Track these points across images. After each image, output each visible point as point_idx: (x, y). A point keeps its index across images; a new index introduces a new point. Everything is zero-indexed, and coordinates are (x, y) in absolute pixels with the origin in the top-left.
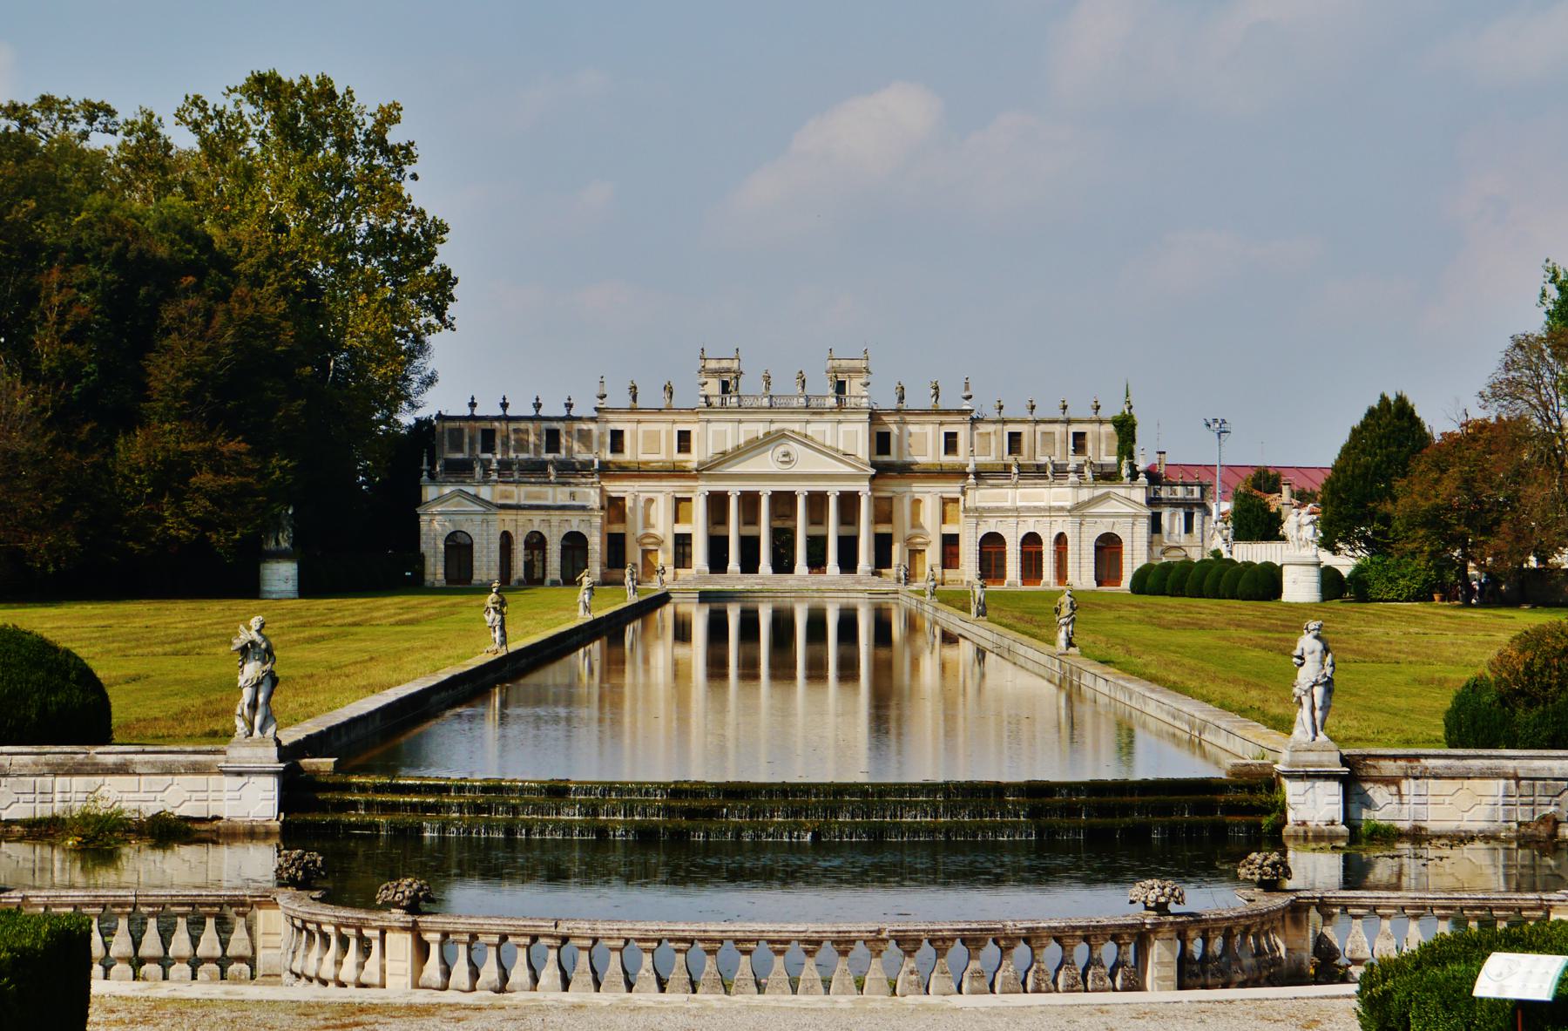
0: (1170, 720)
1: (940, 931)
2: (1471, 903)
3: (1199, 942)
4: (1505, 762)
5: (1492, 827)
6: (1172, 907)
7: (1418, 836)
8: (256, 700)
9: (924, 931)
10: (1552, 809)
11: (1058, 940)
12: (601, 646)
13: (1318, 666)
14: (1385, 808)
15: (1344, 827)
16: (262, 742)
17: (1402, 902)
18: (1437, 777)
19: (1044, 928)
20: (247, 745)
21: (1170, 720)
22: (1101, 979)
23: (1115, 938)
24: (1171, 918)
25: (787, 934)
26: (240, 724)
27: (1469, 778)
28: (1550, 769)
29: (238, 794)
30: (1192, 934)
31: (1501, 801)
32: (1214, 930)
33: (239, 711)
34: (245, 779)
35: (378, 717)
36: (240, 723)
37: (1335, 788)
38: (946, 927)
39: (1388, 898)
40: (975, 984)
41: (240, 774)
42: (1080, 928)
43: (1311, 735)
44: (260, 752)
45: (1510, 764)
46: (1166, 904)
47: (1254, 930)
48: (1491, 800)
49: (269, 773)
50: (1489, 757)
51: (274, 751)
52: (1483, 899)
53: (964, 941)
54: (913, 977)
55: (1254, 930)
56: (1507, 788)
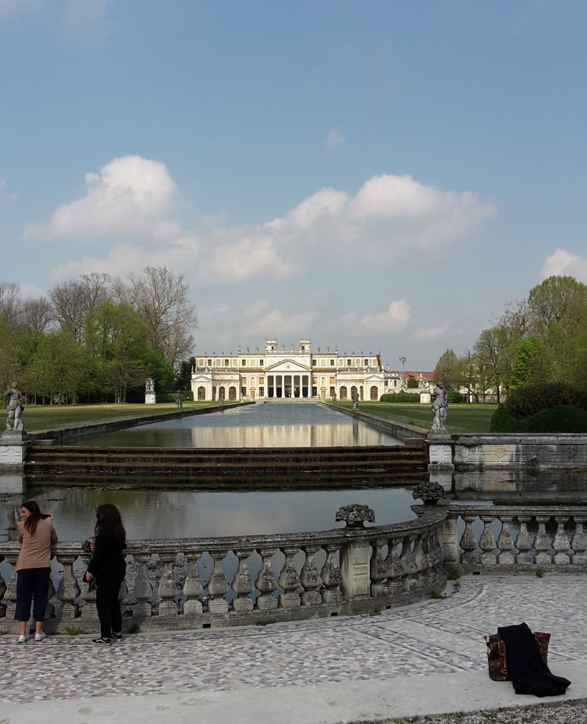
0: (385, 427)
1: (190, 546)
2: (560, 513)
3: (386, 547)
4: (517, 438)
5: (512, 464)
6: (366, 524)
7: (481, 468)
8: (14, 416)
9: (177, 546)
10: (535, 456)
11: (282, 550)
12: (185, 403)
13: (442, 399)
14: (467, 456)
15: (452, 464)
16: (17, 432)
17: (517, 513)
18: (489, 444)
19: (270, 542)
20: (10, 434)
21: (385, 427)
22: (314, 578)
23: (324, 547)
24: (365, 532)
25: (71, 551)
26: (8, 426)
27: (502, 444)
28: (535, 440)
29: (6, 454)
30: (380, 543)
31: (514, 453)
32: (396, 539)
33: (8, 421)
34: (9, 447)
35: (104, 426)
36: (8, 426)
37: (449, 448)
38: (194, 543)
39: (507, 511)
40: (218, 585)
41: (6, 446)
42: (298, 541)
43: (439, 427)
44: (15, 437)
45: (519, 438)
46: (362, 522)
47: (424, 536)
48: (511, 453)
49: (18, 445)
50: (510, 436)
51: (20, 437)
52: (569, 511)
53: (210, 553)
54: (170, 581)
55: (424, 536)
56: (517, 448)
